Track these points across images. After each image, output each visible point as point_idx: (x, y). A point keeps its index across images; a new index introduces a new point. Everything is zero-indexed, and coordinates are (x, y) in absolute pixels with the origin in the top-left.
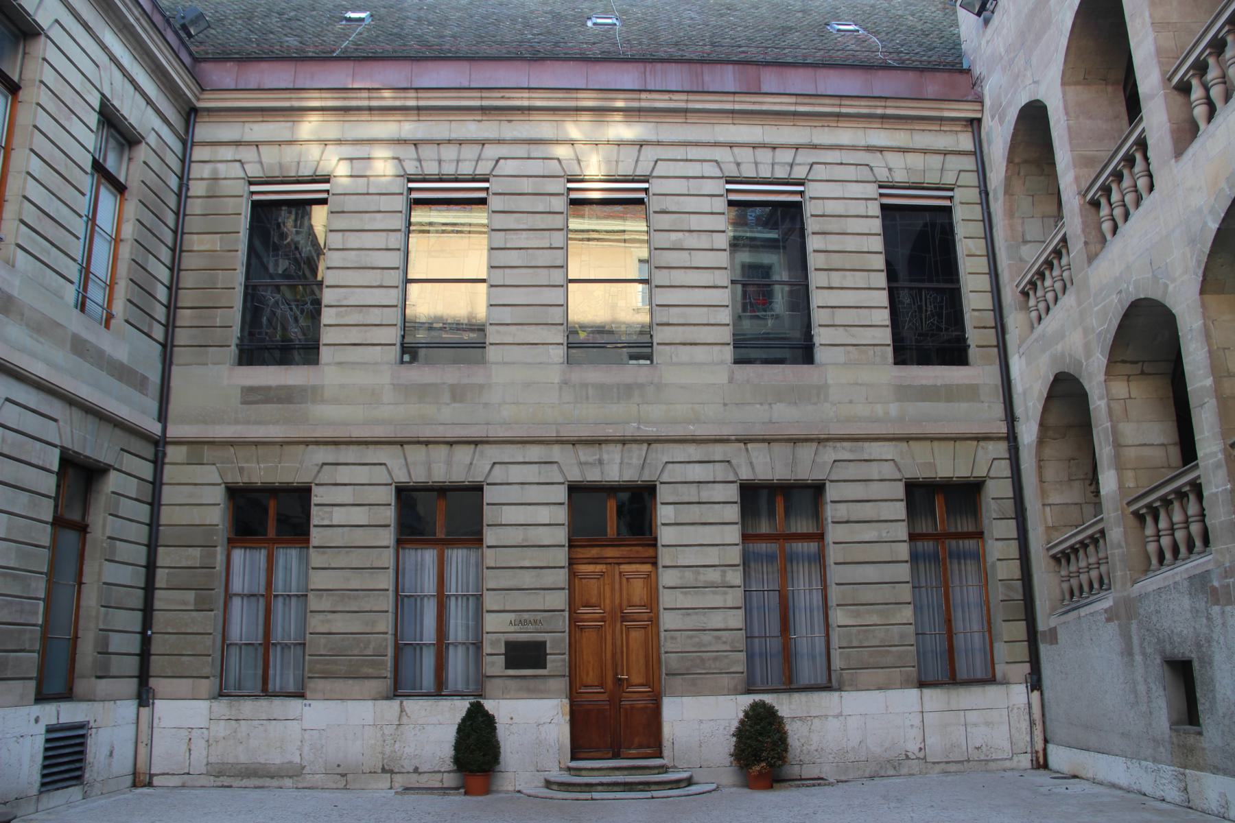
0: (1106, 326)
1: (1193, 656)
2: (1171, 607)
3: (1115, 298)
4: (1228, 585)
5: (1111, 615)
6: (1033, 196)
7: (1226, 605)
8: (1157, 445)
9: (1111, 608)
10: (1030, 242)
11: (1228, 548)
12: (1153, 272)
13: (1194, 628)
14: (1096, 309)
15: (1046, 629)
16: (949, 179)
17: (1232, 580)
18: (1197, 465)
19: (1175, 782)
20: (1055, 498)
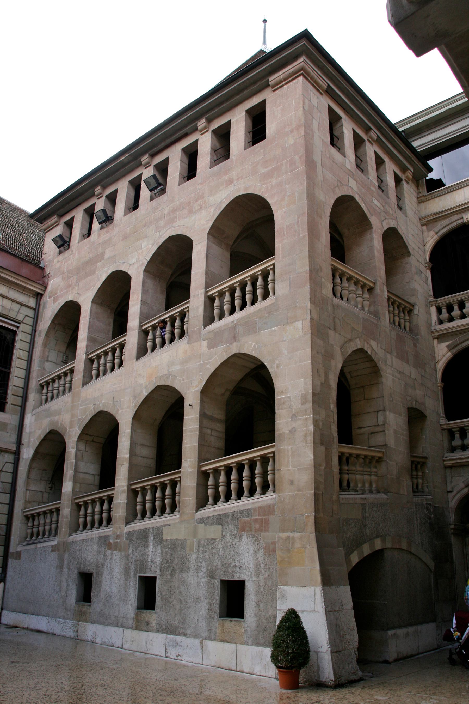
0: (84, 417)
1: (94, 571)
2: (87, 548)
3: (92, 406)
5: (54, 549)
6: (57, 340)
8: (91, 474)
9: (55, 545)
10: (50, 361)
11: (120, 527)
13: (97, 559)
14: (81, 407)
15: (14, 551)
16: (20, 318)
17: (119, 540)
18: (114, 489)
19: (73, 628)
20: (33, 487)
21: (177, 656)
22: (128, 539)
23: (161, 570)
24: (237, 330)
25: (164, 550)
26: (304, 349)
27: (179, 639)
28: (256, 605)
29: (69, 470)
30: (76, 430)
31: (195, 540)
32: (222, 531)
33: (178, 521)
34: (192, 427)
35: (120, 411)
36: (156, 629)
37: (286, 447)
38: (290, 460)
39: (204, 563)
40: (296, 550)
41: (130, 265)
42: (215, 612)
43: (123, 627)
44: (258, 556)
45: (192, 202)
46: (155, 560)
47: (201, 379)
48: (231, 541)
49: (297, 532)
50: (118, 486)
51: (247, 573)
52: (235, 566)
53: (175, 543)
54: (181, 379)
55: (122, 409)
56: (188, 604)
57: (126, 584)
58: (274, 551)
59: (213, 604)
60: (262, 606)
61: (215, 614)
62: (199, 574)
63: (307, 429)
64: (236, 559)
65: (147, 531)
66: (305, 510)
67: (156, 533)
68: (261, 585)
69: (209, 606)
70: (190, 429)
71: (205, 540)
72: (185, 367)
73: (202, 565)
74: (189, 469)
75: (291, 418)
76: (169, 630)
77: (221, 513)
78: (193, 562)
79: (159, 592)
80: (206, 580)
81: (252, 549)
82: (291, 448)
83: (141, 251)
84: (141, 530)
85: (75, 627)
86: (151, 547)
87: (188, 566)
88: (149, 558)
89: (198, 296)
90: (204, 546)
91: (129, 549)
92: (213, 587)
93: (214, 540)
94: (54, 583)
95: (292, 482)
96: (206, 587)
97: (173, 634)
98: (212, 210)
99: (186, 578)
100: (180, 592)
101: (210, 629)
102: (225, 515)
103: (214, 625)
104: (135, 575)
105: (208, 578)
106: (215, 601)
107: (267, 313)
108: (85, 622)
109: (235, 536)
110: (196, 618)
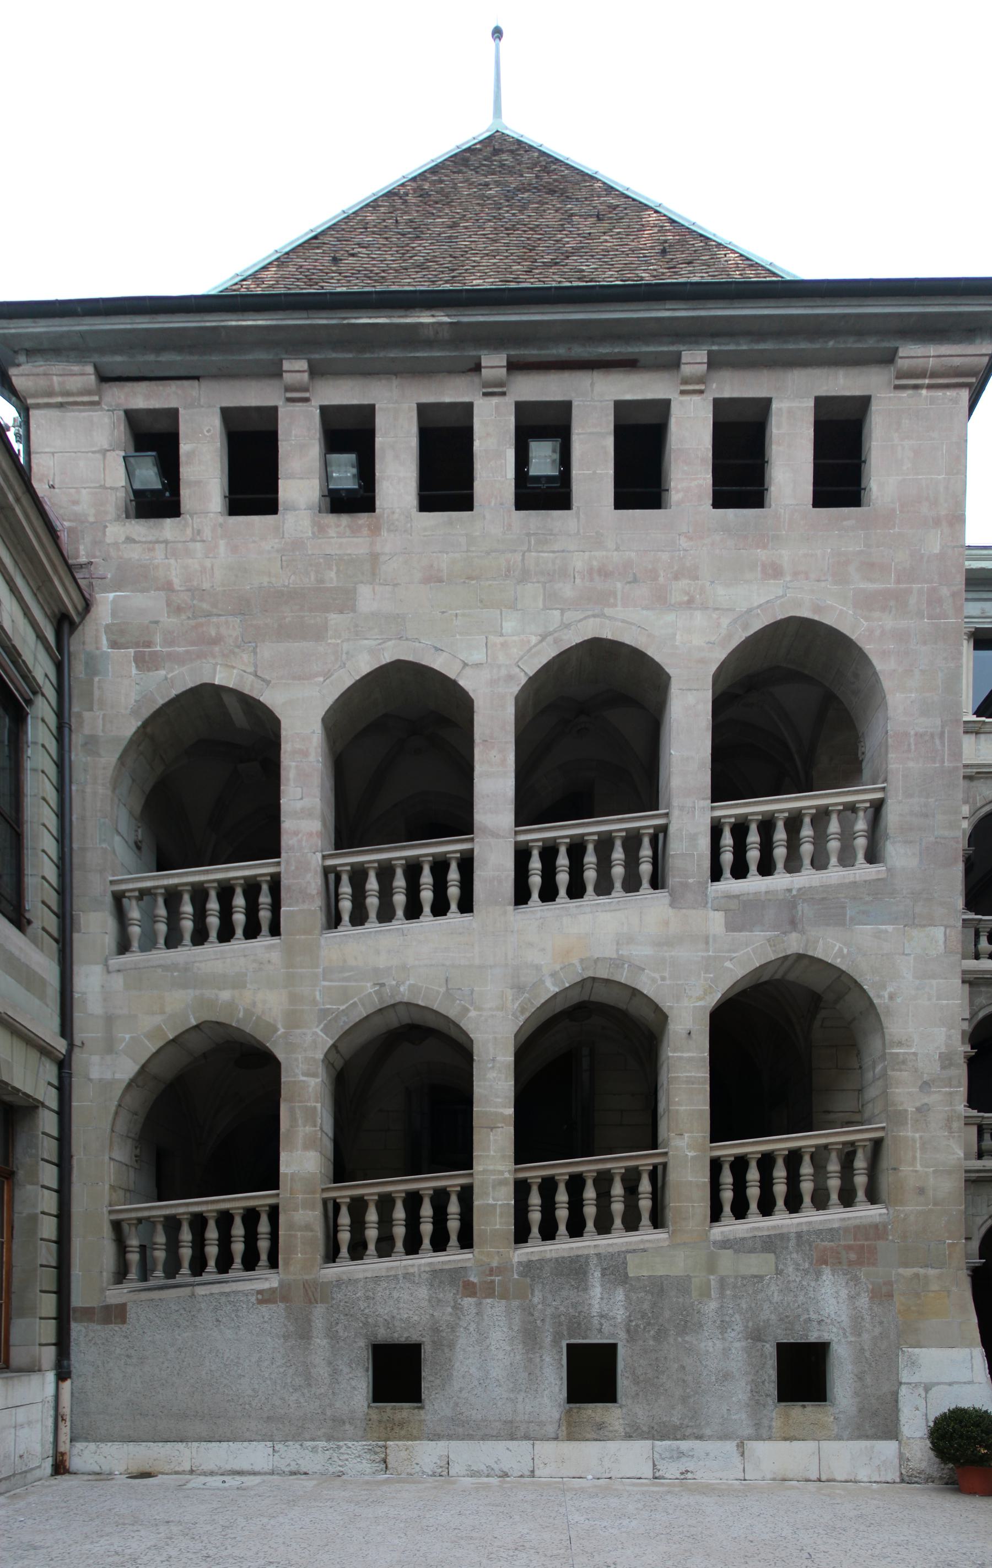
0: (342, 1008)
2: (395, 1294)
3: (369, 988)
4: (493, 1282)
5: (266, 1298)
7: (486, 1298)
9: (273, 1290)
11: (498, 1252)
12: (448, 989)
17: (499, 1278)
21: (682, 1473)
22: (526, 1276)
23: (628, 1331)
24: (799, 908)
25: (634, 1296)
26: (946, 978)
27: (684, 1445)
28: (856, 1379)
29: (300, 1122)
30: (315, 1034)
31: (712, 1277)
32: (776, 1263)
33: (667, 1243)
34: (693, 1074)
35: (473, 1014)
36: (623, 1434)
37: (910, 1134)
38: (918, 1155)
39: (737, 1316)
40: (932, 1295)
41: (465, 665)
42: (767, 1395)
43: (529, 1439)
44: (857, 1304)
45: (662, 574)
46: (611, 1314)
47: (710, 987)
48: (798, 1280)
49: (932, 1267)
50: (485, 1171)
51: (835, 1330)
52: (810, 1320)
53: (662, 1283)
54: (657, 976)
55: (479, 1009)
56: (703, 1387)
57: (530, 1360)
58: (890, 1295)
59: (763, 1382)
60: (868, 1380)
61: (769, 1399)
62: (726, 1335)
63: (952, 1110)
64: (811, 1309)
65: (583, 1260)
66: (947, 1235)
67: (608, 1264)
68: (866, 1348)
69: (753, 1385)
70: (687, 1077)
71: (736, 1277)
72: (667, 954)
73: (733, 1319)
74: (690, 1152)
75: (921, 1087)
76: (658, 1432)
77: (772, 1233)
78: (710, 1315)
79: (628, 1369)
80: (744, 1344)
81: (844, 1293)
82: (921, 1138)
83: (501, 639)
84: (563, 1258)
85: (376, 1453)
86: (596, 1291)
87: (700, 1323)
88: (594, 1310)
89: (693, 812)
90: (735, 1287)
91: (532, 1294)
92: (762, 1355)
93: (761, 1278)
94: (282, 1370)
95: (921, 1191)
96: (745, 1356)
97: (669, 1439)
98: (725, 622)
99: (695, 1342)
100: (683, 1367)
101: (757, 1422)
102: (783, 1237)
103: (765, 1415)
104: (556, 1342)
105: (749, 1341)
106: (767, 1378)
107: (869, 895)
108: (408, 1440)
109: (806, 1272)
110: (725, 1408)
